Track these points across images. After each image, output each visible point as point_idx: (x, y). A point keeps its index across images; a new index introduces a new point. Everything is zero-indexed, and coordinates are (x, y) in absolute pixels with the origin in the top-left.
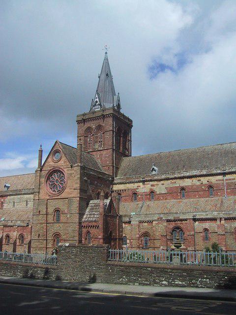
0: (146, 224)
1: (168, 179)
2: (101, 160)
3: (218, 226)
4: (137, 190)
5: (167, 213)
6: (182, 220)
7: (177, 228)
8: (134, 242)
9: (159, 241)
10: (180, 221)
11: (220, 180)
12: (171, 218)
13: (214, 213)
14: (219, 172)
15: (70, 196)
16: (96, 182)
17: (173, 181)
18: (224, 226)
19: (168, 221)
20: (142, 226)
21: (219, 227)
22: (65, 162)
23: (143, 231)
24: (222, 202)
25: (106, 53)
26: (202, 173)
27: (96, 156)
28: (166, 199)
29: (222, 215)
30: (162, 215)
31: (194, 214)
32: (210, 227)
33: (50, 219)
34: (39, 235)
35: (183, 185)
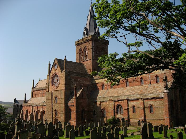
0: (104, 103)
4: (104, 83)
6: (121, 100)
12: (116, 99)
13: (138, 95)
15: (61, 89)
16: (79, 80)
19: (115, 101)
22: (59, 70)
24: (147, 87)
27: (85, 63)
28: (119, 88)
29: (142, 97)
30: (111, 98)
31: (127, 96)
32: (136, 104)
33: (53, 101)
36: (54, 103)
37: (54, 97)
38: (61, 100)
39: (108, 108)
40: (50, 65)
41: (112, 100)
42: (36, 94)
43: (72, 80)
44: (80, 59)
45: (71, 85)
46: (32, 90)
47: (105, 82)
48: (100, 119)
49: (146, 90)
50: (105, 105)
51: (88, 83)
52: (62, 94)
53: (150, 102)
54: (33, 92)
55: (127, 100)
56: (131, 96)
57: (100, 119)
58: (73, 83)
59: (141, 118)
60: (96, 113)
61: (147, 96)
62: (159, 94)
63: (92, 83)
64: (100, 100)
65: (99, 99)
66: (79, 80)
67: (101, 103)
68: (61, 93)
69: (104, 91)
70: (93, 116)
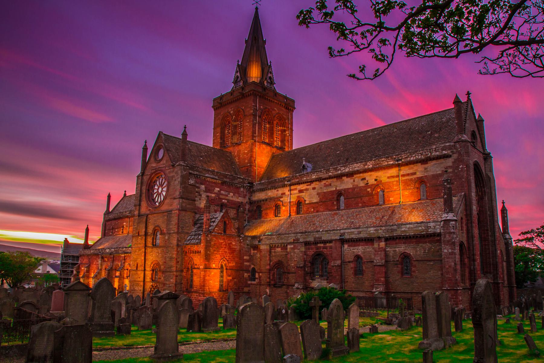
0: (279, 249)
1: (319, 180)
2: (239, 158)
3: (376, 251)
5: (306, 232)
6: (325, 242)
7: (318, 255)
8: (265, 278)
9: (294, 275)
10: (323, 243)
11: (393, 177)
12: (311, 239)
13: (369, 230)
14: (391, 163)
15: (171, 208)
16: (217, 189)
17: (327, 183)
18: (385, 250)
19: (307, 244)
20: (275, 252)
21: (376, 251)
22: (167, 161)
23: (275, 259)
25: (257, 9)
26: (366, 167)
28: (317, 211)
31: (342, 231)
32: (364, 253)
33: (150, 240)
34: (137, 265)
35: (341, 188)
36: (151, 246)
37: (150, 230)
38: (169, 238)
39: (290, 262)
40: (145, 149)
41: (301, 240)
42: (114, 226)
43: (198, 188)
44: (224, 141)
45: (195, 200)
46: (104, 218)
47: (282, 197)
48: (268, 291)
49: (390, 216)
50: (281, 255)
51: (240, 199)
52: (173, 222)
53: (401, 248)
54: (107, 223)
55: (338, 244)
56: (353, 230)
57: (268, 291)
58: (203, 195)
59: (377, 288)
60: (257, 276)
61: (396, 230)
62: (429, 225)
63: (249, 199)
64: (267, 242)
65: (266, 240)
66: (219, 189)
67: (271, 248)
68: (169, 221)
69: (280, 220)
70: (249, 282)
